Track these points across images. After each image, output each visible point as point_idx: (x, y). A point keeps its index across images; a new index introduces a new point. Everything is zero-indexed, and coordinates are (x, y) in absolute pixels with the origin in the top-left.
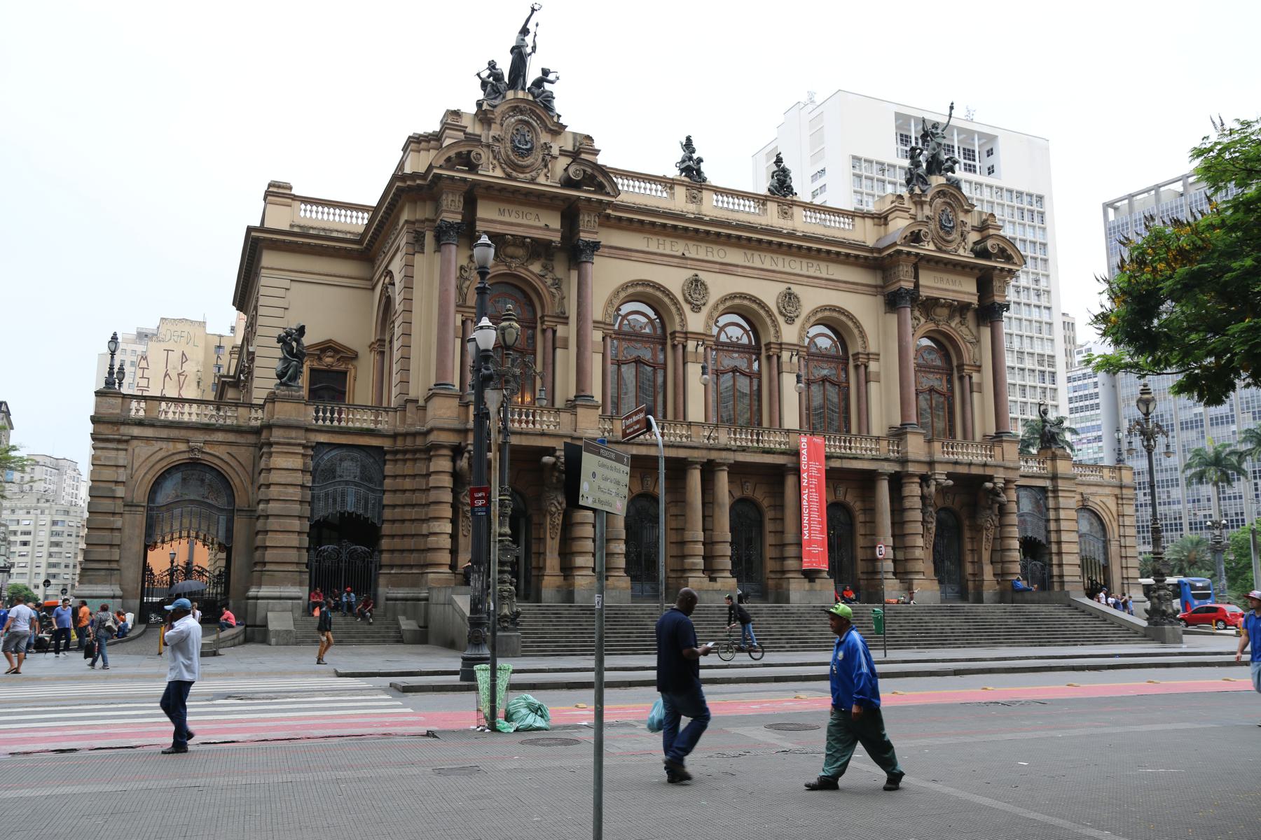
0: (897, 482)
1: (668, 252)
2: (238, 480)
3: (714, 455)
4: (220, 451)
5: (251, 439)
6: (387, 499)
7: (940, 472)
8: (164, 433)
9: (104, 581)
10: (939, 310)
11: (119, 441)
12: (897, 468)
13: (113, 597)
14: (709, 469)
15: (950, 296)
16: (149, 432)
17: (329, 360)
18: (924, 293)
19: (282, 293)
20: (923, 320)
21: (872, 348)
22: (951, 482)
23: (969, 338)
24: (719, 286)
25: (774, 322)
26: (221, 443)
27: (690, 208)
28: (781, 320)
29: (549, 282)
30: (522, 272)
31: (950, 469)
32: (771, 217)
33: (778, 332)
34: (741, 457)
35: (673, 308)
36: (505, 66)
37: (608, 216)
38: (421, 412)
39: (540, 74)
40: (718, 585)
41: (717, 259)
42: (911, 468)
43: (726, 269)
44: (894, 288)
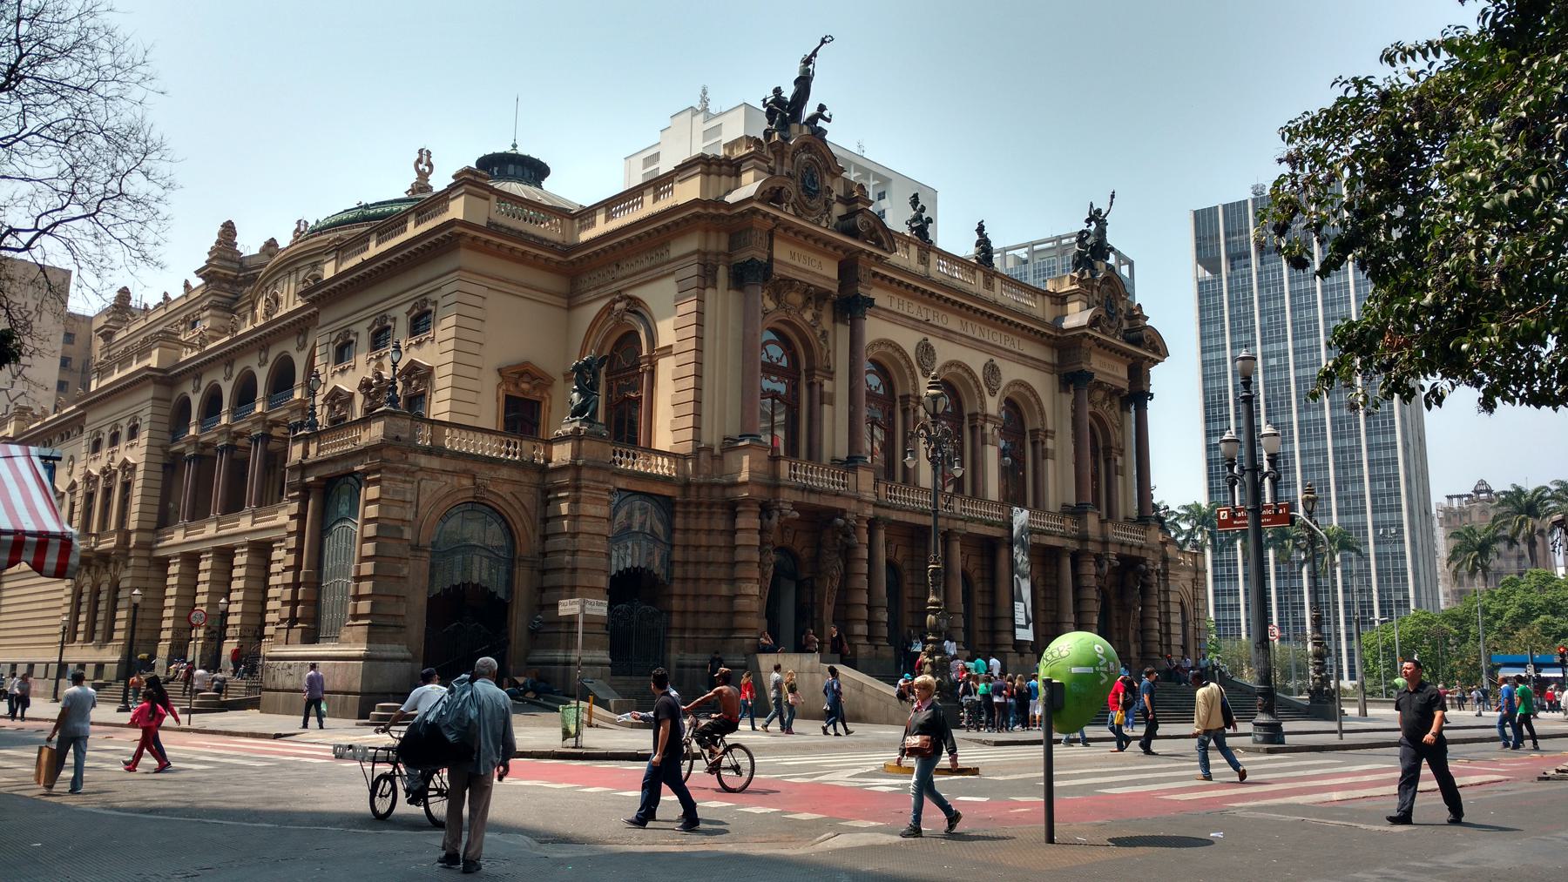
0: (1076, 558)
2: (522, 525)
4: (505, 490)
5: (535, 478)
6: (678, 555)
8: (451, 465)
9: (394, 641)
11: (407, 472)
13: (403, 660)
15: (1110, 381)
16: (435, 463)
17: (524, 386)
19: (478, 301)
21: (1050, 427)
24: (945, 352)
25: (981, 392)
26: (505, 481)
28: (986, 390)
29: (819, 333)
30: (798, 322)
32: (976, 284)
33: (983, 404)
35: (907, 371)
36: (788, 93)
38: (717, 463)
39: (815, 111)
43: (948, 335)
44: (1075, 368)
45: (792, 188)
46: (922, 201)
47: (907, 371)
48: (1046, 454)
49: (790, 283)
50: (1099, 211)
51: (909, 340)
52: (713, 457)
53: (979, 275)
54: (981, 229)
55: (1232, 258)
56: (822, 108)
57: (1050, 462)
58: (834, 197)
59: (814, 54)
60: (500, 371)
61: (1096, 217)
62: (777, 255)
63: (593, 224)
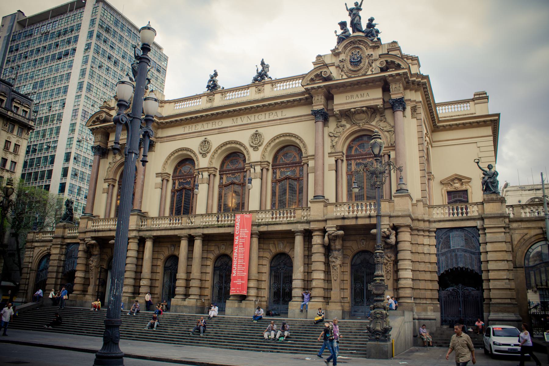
1: (194, 131)
3: (192, 232)
7: (331, 227)
10: (357, 116)
12: (306, 227)
14: (191, 240)
15: (358, 105)
18: (337, 109)
20: (348, 126)
22: (342, 232)
23: (388, 128)
27: (208, 105)
31: (340, 223)
34: (206, 231)
37: (162, 123)
40: (186, 303)
41: (217, 127)
42: (313, 226)
43: (221, 130)
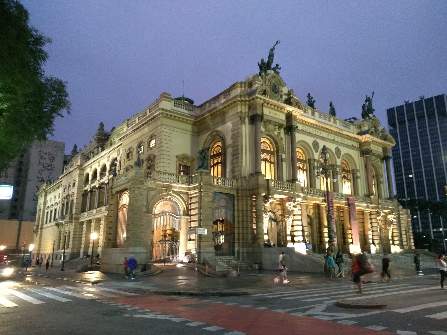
17: (185, 161)
21: (358, 169)
33: (336, 161)
35: (310, 151)
36: (266, 60)
43: (323, 138)
45: (268, 89)
46: (311, 95)
47: (310, 151)
48: (357, 178)
49: (270, 122)
50: (369, 98)
51: (310, 140)
52: (246, 180)
53: (332, 119)
54: (331, 105)
55: (400, 123)
56: (277, 65)
57: (359, 180)
58: (283, 94)
59: (274, 48)
60: (176, 156)
61: (368, 100)
62: (265, 112)
63: (205, 109)
